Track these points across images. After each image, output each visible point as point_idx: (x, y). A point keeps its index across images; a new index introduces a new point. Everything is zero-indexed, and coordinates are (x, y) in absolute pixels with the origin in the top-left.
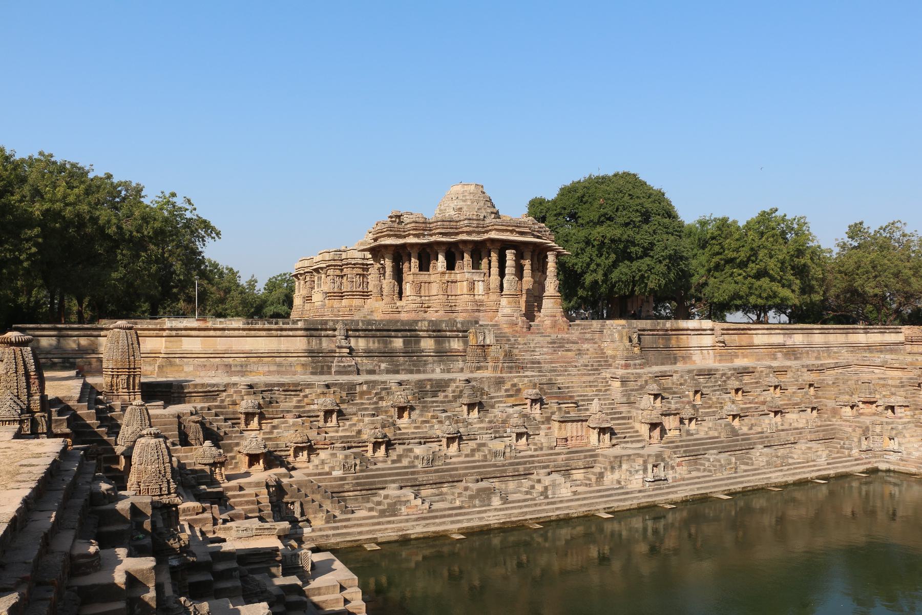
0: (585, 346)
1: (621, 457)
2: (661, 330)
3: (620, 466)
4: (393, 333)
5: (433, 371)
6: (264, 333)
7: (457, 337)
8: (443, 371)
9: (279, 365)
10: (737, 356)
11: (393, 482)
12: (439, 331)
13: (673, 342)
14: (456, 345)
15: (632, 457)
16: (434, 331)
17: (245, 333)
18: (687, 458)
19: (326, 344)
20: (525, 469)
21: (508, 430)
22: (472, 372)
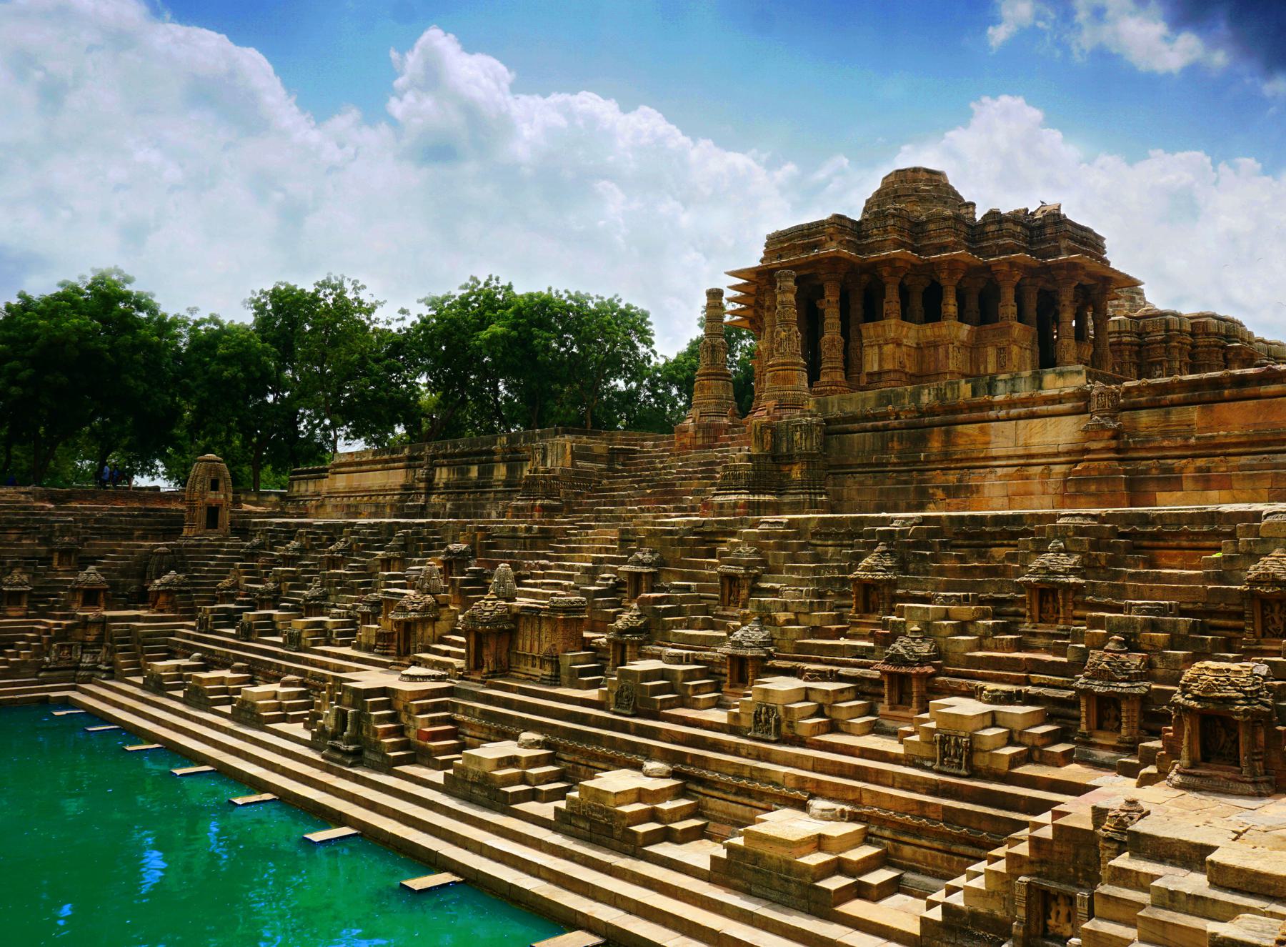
10: (1171, 481)
13: (935, 445)
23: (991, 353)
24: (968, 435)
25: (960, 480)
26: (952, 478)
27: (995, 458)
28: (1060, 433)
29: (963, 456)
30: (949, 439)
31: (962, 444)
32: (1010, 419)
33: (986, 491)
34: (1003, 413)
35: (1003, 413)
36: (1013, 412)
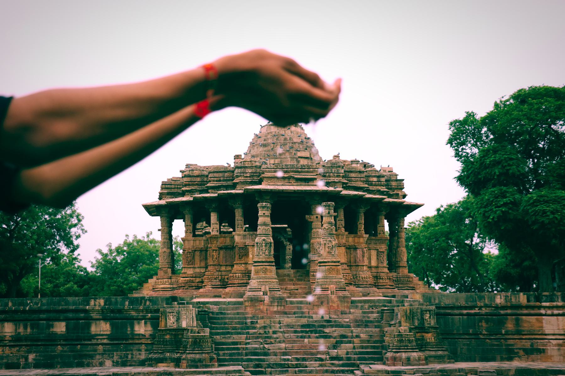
0: (356, 331)
2: (486, 306)
5: (101, 364)
7: (144, 318)
8: (116, 364)
12: (120, 311)
13: (510, 326)
14: (141, 329)
22: (151, 365)
23: (374, 253)
24: (529, 322)
25: (532, 345)
26: (527, 344)
27: (546, 335)
29: (528, 333)
30: (518, 322)
31: (525, 327)
32: (553, 315)
33: (549, 352)
34: (549, 312)
35: (549, 312)
36: (556, 312)
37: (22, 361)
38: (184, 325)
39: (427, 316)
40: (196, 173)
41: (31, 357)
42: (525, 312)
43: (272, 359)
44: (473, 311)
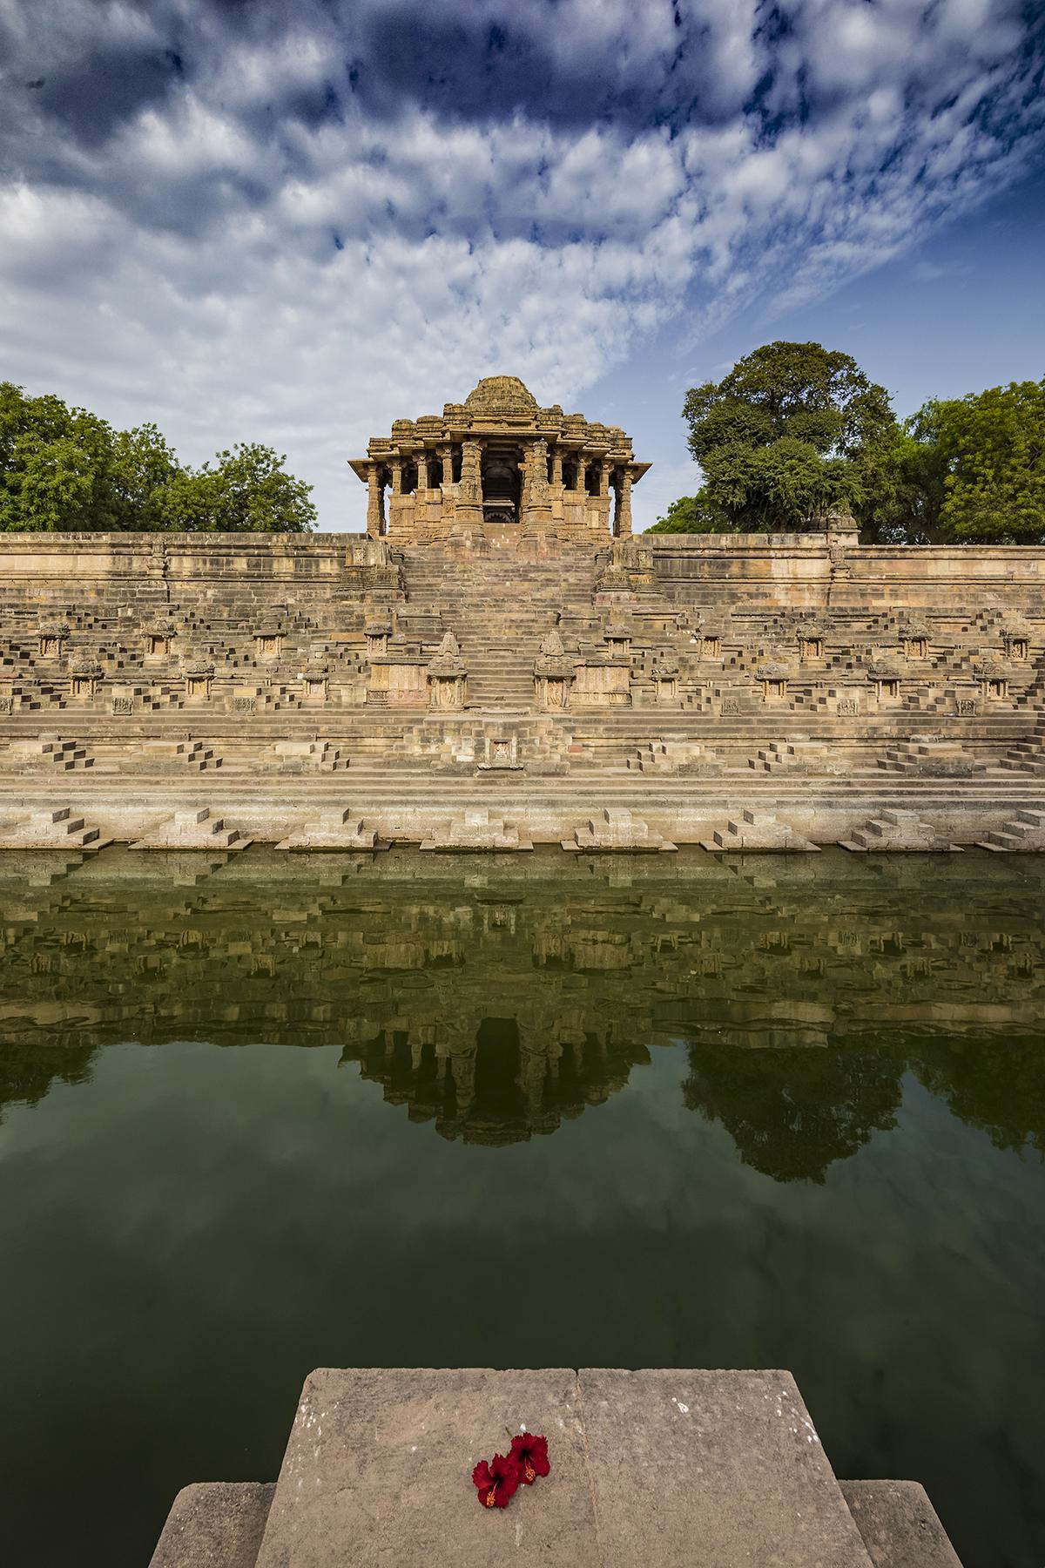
0: (564, 575)
1: (442, 723)
3: (442, 741)
4: (233, 551)
6: (55, 550)
7: (330, 556)
9: (67, 591)
11: (50, 729)
12: (304, 548)
13: (735, 569)
15: (467, 726)
16: (296, 548)
17: (29, 549)
18: (612, 742)
19: (137, 564)
20: (276, 730)
21: (300, 676)
26: (753, 588)
28: (815, 568)
34: (779, 554)
36: (786, 554)
37: (201, 596)
38: (372, 562)
39: (643, 556)
40: (404, 426)
41: (210, 593)
42: (752, 553)
43: (469, 600)
44: (694, 554)
